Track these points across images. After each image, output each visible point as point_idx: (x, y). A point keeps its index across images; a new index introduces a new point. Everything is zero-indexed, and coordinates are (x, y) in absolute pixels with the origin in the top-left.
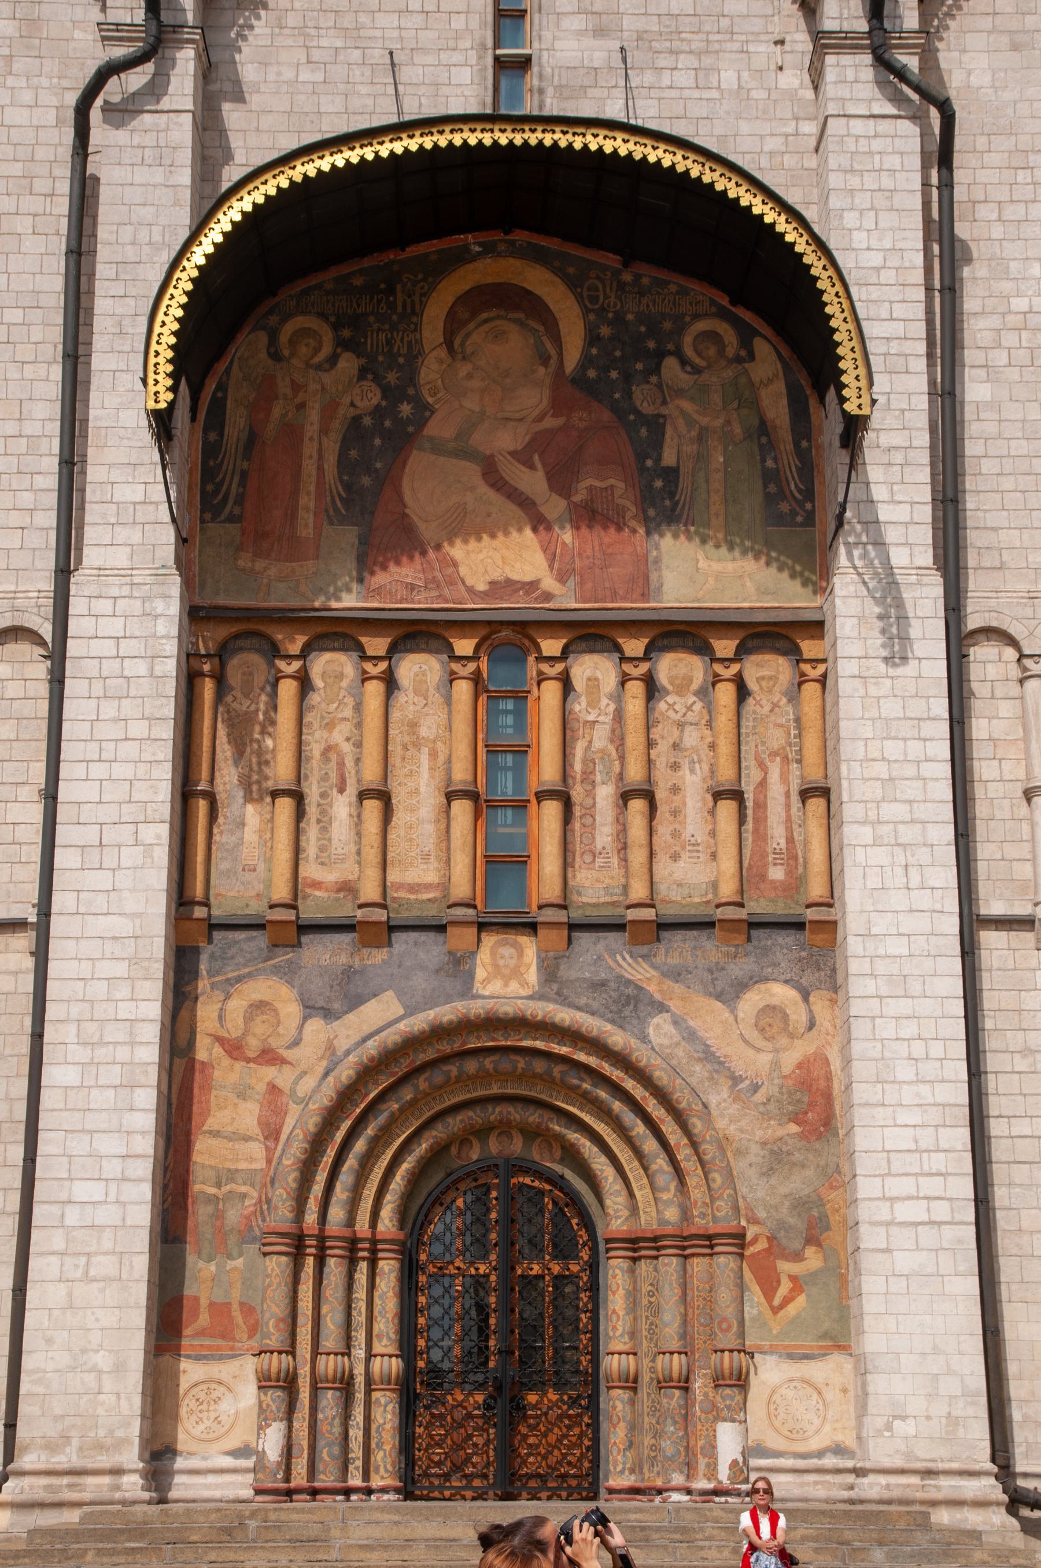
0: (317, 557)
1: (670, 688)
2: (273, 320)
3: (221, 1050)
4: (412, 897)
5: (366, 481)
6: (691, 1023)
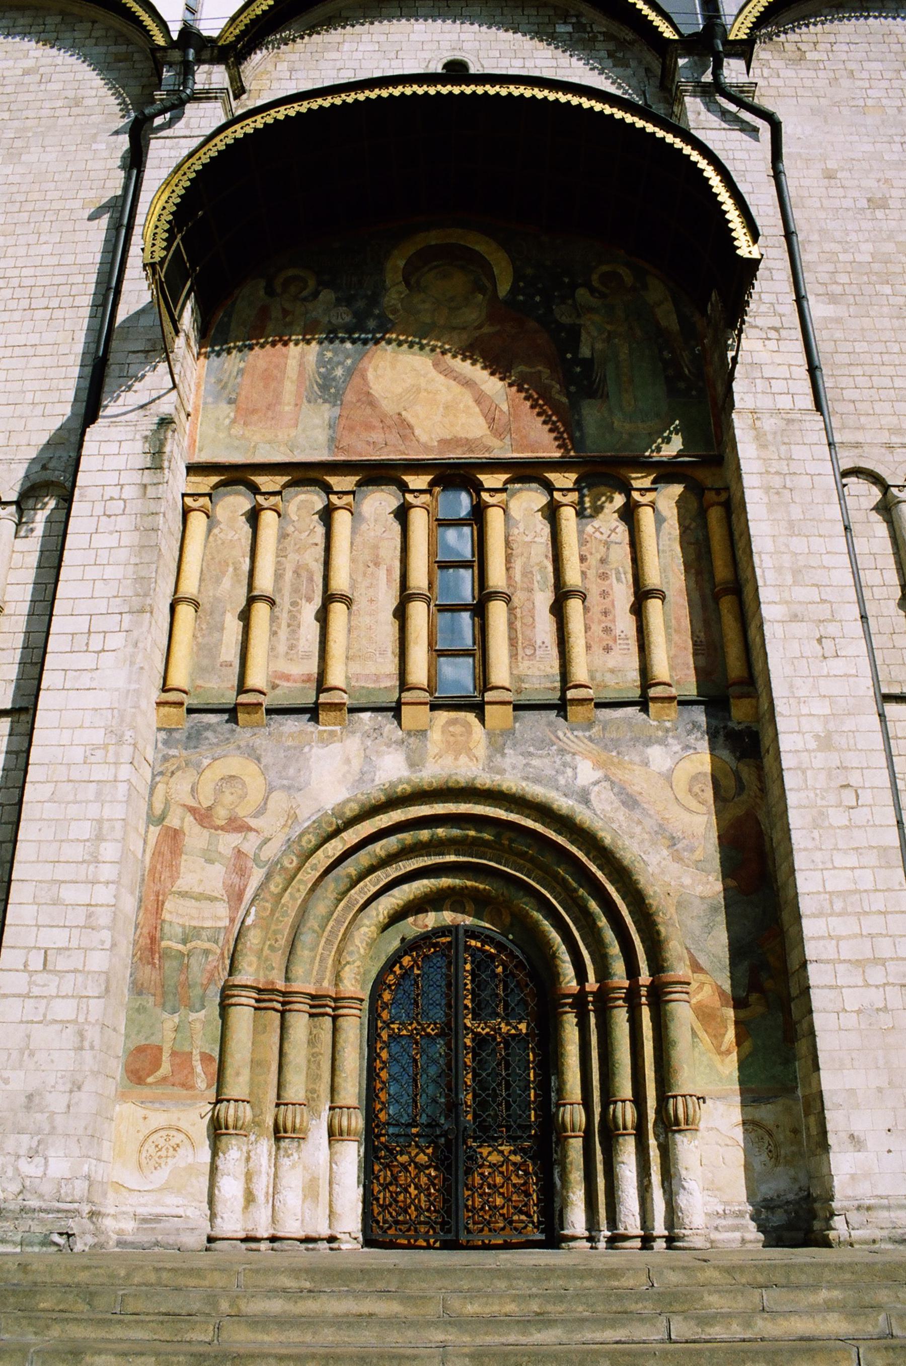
3: (192, 818)
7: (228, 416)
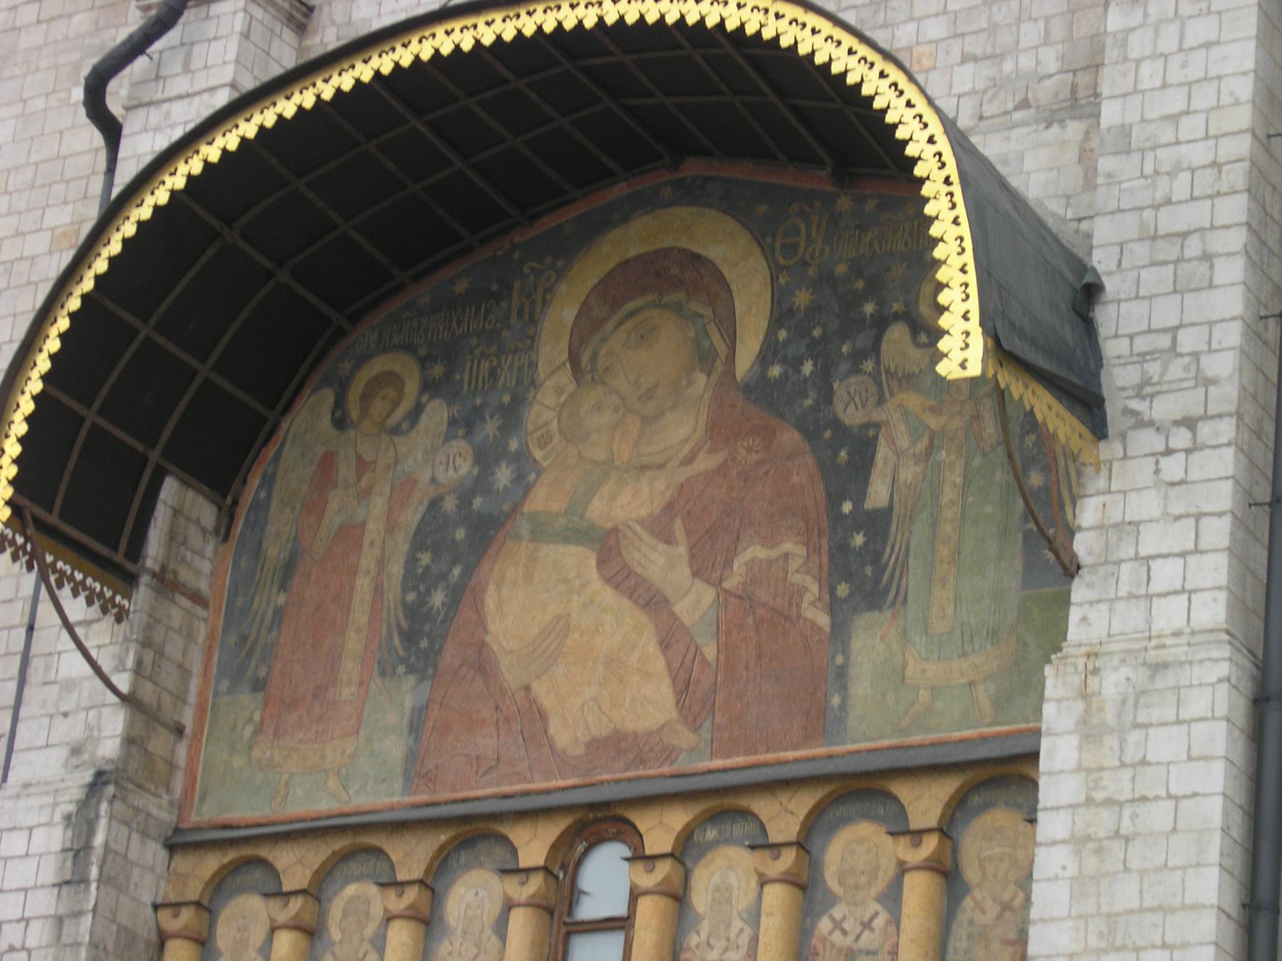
2: (347, 366)
7: (250, 720)
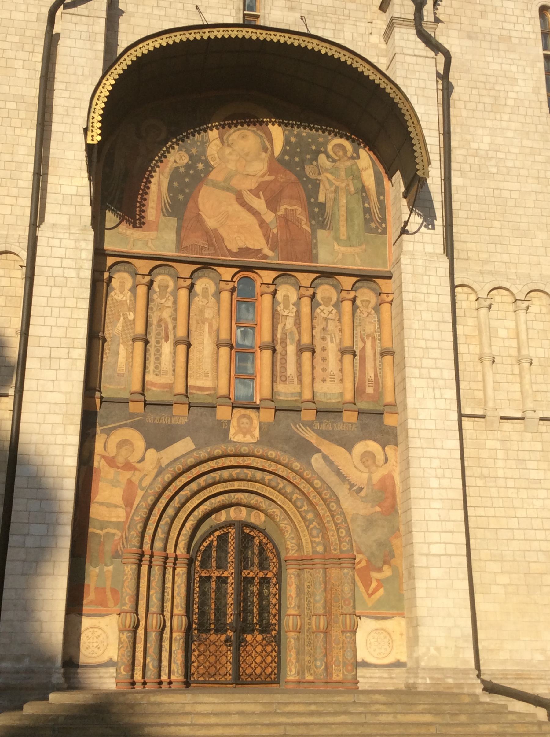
0: (157, 230)
1: (321, 302)
3: (105, 462)
4: (199, 393)
5: (181, 197)
6: (331, 458)
